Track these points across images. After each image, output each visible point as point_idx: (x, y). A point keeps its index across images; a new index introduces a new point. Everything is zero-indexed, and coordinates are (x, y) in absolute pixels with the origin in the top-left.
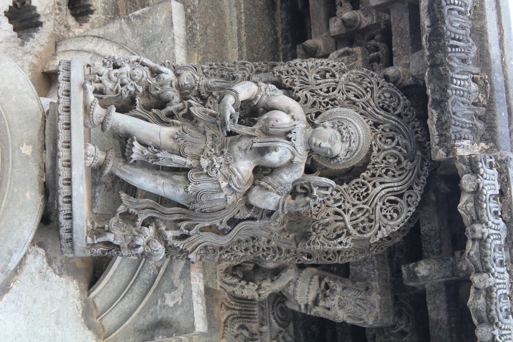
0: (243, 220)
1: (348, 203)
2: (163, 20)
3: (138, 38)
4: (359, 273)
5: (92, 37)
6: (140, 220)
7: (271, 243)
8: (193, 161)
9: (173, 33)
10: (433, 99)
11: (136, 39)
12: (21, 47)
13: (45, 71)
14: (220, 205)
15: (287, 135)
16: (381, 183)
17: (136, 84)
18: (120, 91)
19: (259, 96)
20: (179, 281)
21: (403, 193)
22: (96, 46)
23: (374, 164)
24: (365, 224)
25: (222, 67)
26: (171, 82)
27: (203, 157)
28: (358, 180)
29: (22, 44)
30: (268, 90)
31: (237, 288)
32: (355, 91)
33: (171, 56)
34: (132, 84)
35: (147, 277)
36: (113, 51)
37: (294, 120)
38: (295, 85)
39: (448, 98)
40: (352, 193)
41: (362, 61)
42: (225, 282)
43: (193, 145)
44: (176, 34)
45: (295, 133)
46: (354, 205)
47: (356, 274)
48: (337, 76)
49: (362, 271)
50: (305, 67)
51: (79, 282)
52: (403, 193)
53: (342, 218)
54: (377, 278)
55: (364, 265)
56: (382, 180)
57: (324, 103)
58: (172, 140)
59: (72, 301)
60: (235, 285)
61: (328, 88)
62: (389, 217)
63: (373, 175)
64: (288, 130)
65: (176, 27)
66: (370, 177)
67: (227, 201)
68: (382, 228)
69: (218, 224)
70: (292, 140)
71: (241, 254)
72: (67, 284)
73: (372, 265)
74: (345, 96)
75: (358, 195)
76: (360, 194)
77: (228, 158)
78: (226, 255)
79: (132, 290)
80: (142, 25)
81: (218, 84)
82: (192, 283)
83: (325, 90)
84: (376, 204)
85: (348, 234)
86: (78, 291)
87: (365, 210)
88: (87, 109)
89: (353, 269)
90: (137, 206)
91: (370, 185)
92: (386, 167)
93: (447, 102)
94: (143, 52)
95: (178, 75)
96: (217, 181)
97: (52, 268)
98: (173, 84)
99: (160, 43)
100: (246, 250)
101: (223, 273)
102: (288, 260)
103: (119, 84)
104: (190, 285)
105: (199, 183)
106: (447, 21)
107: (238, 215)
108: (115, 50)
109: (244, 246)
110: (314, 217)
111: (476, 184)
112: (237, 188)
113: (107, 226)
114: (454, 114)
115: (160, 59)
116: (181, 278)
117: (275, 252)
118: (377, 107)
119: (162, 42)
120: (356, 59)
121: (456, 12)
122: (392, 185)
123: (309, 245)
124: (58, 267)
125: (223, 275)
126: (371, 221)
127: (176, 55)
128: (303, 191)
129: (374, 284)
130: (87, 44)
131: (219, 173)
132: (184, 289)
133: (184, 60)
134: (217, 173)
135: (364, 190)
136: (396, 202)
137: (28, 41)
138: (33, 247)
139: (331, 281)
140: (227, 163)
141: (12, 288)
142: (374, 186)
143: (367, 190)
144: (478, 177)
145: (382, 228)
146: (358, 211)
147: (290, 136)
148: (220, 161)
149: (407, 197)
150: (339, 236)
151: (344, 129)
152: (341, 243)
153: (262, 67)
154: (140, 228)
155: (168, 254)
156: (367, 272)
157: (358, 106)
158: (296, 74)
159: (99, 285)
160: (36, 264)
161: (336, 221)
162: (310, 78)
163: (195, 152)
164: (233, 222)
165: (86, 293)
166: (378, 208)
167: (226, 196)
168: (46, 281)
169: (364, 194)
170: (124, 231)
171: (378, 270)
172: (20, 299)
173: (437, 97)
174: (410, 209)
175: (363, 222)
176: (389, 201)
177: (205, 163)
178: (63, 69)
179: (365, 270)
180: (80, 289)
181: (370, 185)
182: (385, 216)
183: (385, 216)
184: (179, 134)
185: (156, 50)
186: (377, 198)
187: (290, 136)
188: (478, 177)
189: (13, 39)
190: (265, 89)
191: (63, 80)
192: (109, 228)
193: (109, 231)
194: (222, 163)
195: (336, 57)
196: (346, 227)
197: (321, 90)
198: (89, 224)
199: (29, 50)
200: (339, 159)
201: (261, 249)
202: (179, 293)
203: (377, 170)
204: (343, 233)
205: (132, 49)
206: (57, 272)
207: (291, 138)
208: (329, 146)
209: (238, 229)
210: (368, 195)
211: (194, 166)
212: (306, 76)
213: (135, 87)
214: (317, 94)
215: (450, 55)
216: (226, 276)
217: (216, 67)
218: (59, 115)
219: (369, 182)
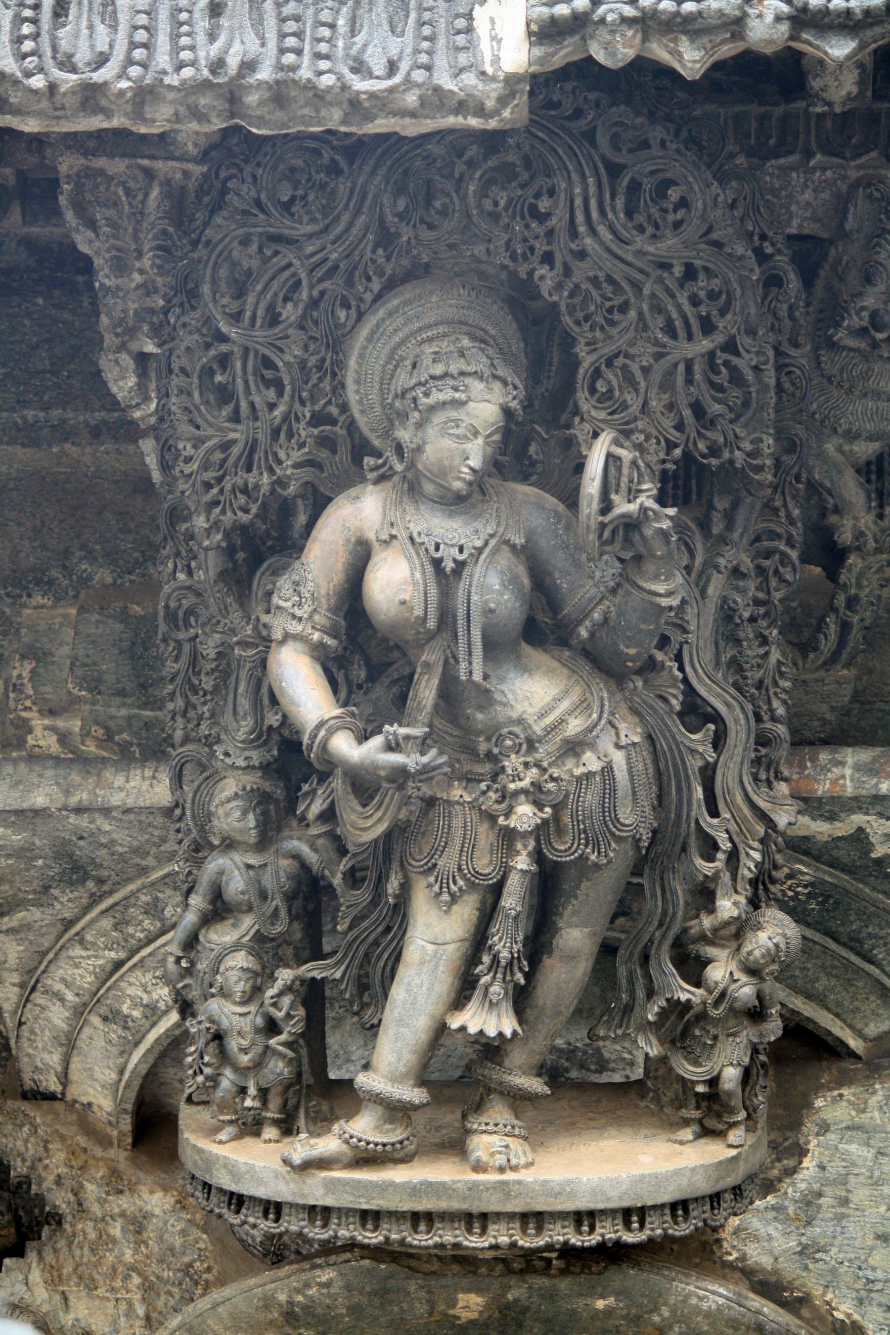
0: (685, 680)
1: (632, 344)
2: (9, 832)
3: (55, 892)
4: (814, 212)
5: (29, 1006)
6: (685, 992)
7: (743, 569)
8: (519, 846)
9: (59, 810)
10: (344, 122)
11: (56, 899)
12: (67, 1226)
13: (130, 1140)
14: (643, 762)
15: (445, 575)
16: (573, 233)
17: (270, 992)
18: (291, 1039)
19: (316, 636)
20: (838, 824)
21: (604, 159)
22: (62, 1000)
23: (514, 257)
24: (702, 294)
25: (179, 680)
26: (249, 867)
27: (507, 815)
28: (563, 308)
29: (56, 1219)
30: (298, 612)
31: (855, 619)
32: (276, 294)
33: (132, 817)
34: (274, 1005)
35: (818, 904)
36: (89, 957)
37: (393, 537)
38: (257, 487)
39: (345, 87)
40: (602, 329)
41: (111, 156)
42: (834, 658)
43: (469, 848)
44: (60, 799)
45: (437, 548)
46: (642, 324)
47: (815, 219)
48: (224, 348)
49: (808, 203)
50: (195, 447)
51: (819, 1089)
52: (604, 159)
53: (681, 368)
54: (836, 160)
55: (790, 197)
56: (562, 235)
57: (313, 399)
58: (455, 908)
59: (877, 1114)
60: (845, 627)
61: (267, 383)
62: (680, 215)
63: (548, 258)
64: (429, 569)
65: (39, 800)
66: (552, 269)
67: (634, 744)
68: (714, 236)
69: (700, 763)
70: (460, 558)
71: (775, 655)
72: (824, 1128)
73: (794, 175)
74: (290, 331)
75: (610, 311)
76: (608, 304)
77: (509, 743)
78: (776, 704)
79: (851, 939)
80: (11, 882)
81: (245, 704)
82: (850, 790)
83: (271, 394)
84: (640, 253)
85: (731, 347)
86: (845, 1091)
87: (662, 295)
88: (366, 1158)
89: (800, 226)
90: (641, 993)
91: (581, 271)
92: (523, 218)
93: (358, 93)
94: (100, 881)
95: (229, 844)
96: (579, 779)
97: (780, 1180)
98: (254, 860)
99: (82, 843)
100: (764, 641)
101: (805, 657)
102: (796, 512)
103: (272, 1042)
104: (856, 798)
105: (585, 831)
106: (98, 77)
107: (674, 702)
108: (84, 953)
109: (752, 651)
110: (678, 452)
111: (624, 27)
112: (600, 717)
113: (700, 1089)
114: (392, 67)
115: (135, 843)
116: (832, 817)
117: (768, 554)
118: (326, 229)
119: (81, 838)
120: (102, 172)
121: (61, 33)
122: (578, 201)
123: (759, 469)
124: (779, 1160)
125: (812, 655)
126: (690, 273)
127: (130, 802)
128: (621, 532)
129: (854, 175)
130: (48, 1020)
131: (556, 772)
132: (867, 814)
133: (138, 772)
134: (553, 779)
135: (594, 293)
136: (635, 187)
137: (40, 1200)
138: (725, 1244)
139: (846, 323)
140: (524, 747)
141: (849, 1316)
142: (582, 255)
143: (594, 281)
144: (603, 21)
145: (714, 236)
146: (660, 312)
147: (449, 565)
148: (521, 768)
149: (619, 150)
150: (736, 377)
151: (427, 395)
152: (756, 369)
153: (178, 554)
154: (710, 992)
155: (770, 877)
156: (815, 191)
157: (322, 293)
158: (219, 480)
159: (830, 1033)
160: (775, 1234)
161: (689, 381)
162: (233, 436)
163: (485, 837)
164: (696, 712)
165: (849, 1065)
166: (651, 249)
167: (618, 746)
168: (822, 1201)
169: (608, 290)
170: (715, 1038)
171: (809, 154)
172: (879, 1286)
173: (336, 114)
174: (655, 143)
175: (695, 301)
176: (629, 214)
177: (525, 815)
178: (238, 1212)
179: (808, 196)
180: (840, 1085)
181: (577, 267)
182: (677, 225)
183: (677, 225)
184: (436, 888)
185: (103, 852)
186: (620, 252)
187: (449, 565)
188: (603, 21)
189: (50, 1258)
190: (294, 616)
191: (277, 1220)
192: (704, 1082)
193: (714, 1082)
194: (526, 765)
195: (91, 234)
196: (711, 355)
197: (272, 406)
198: (687, 1134)
199: (72, 1198)
200: (514, 404)
201: (761, 595)
202: (875, 825)
203: (532, 249)
204: (726, 363)
205: (86, 910)
206: (789, 1163)
207: (455, 560)
208: (480, 441)
209: (706, 685)
210: (610, 280)
211: (532, 844)
212: (226, 446)
213: (281, 994)
214: (286, 418)
215: (206, 73)
216: (816, 649)
217: (180, 703)
218: (387, 1239)
219: (567, 271)
